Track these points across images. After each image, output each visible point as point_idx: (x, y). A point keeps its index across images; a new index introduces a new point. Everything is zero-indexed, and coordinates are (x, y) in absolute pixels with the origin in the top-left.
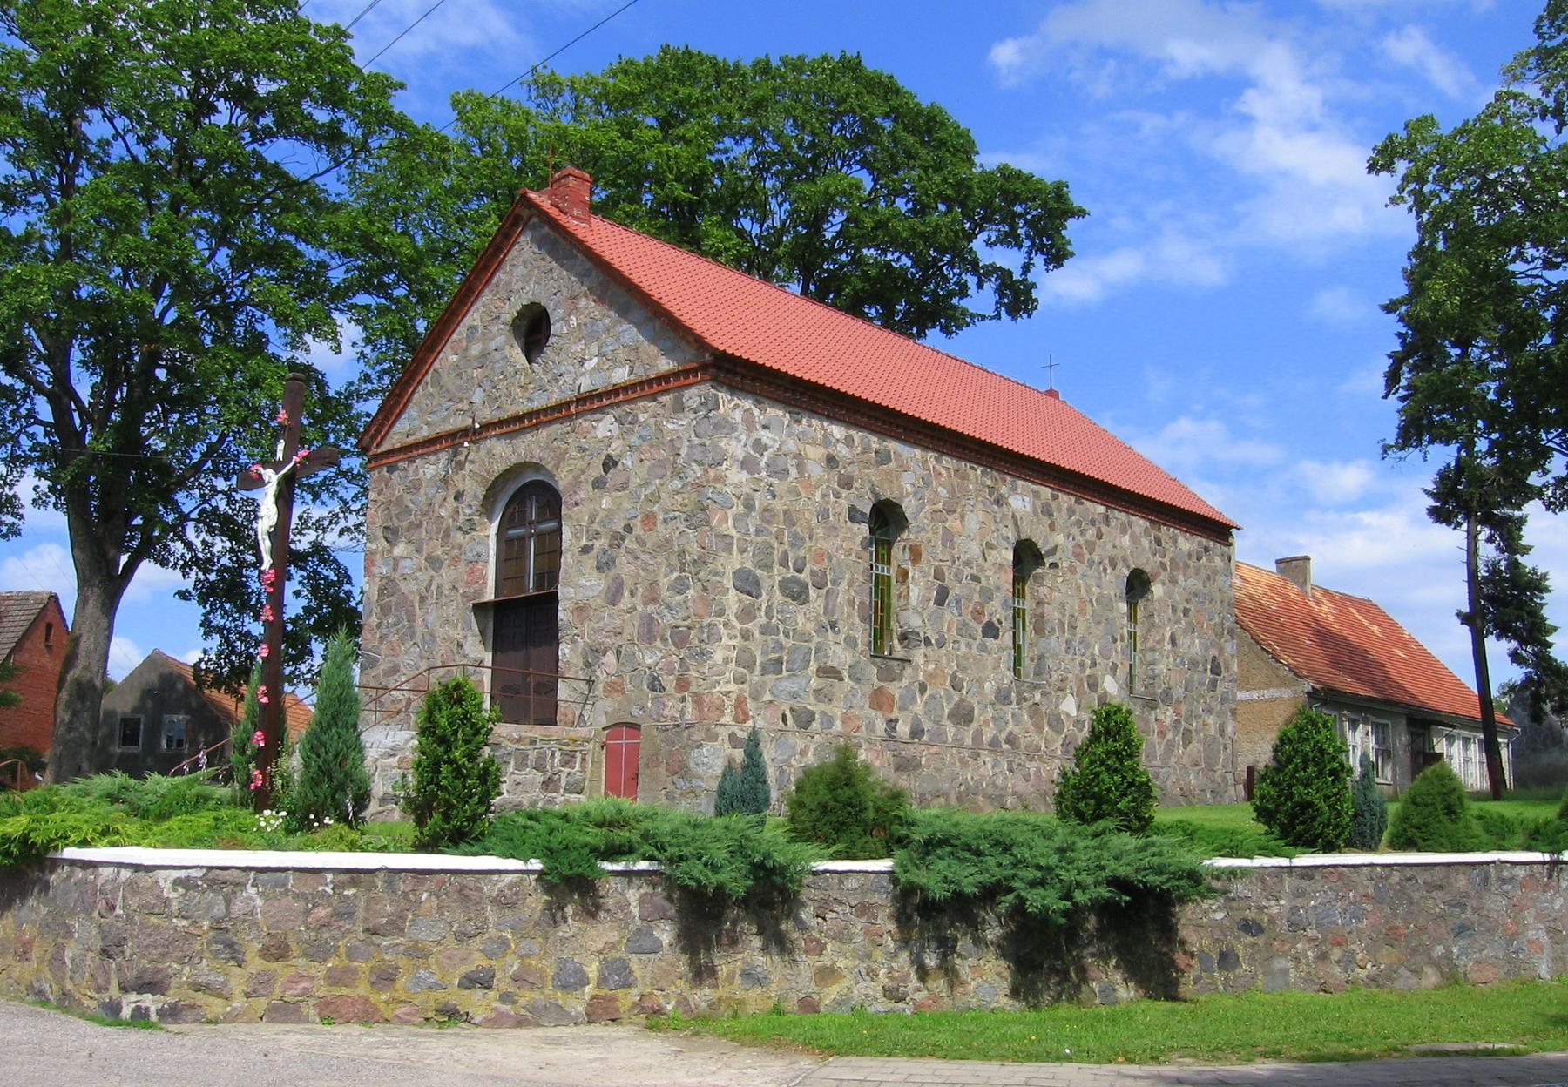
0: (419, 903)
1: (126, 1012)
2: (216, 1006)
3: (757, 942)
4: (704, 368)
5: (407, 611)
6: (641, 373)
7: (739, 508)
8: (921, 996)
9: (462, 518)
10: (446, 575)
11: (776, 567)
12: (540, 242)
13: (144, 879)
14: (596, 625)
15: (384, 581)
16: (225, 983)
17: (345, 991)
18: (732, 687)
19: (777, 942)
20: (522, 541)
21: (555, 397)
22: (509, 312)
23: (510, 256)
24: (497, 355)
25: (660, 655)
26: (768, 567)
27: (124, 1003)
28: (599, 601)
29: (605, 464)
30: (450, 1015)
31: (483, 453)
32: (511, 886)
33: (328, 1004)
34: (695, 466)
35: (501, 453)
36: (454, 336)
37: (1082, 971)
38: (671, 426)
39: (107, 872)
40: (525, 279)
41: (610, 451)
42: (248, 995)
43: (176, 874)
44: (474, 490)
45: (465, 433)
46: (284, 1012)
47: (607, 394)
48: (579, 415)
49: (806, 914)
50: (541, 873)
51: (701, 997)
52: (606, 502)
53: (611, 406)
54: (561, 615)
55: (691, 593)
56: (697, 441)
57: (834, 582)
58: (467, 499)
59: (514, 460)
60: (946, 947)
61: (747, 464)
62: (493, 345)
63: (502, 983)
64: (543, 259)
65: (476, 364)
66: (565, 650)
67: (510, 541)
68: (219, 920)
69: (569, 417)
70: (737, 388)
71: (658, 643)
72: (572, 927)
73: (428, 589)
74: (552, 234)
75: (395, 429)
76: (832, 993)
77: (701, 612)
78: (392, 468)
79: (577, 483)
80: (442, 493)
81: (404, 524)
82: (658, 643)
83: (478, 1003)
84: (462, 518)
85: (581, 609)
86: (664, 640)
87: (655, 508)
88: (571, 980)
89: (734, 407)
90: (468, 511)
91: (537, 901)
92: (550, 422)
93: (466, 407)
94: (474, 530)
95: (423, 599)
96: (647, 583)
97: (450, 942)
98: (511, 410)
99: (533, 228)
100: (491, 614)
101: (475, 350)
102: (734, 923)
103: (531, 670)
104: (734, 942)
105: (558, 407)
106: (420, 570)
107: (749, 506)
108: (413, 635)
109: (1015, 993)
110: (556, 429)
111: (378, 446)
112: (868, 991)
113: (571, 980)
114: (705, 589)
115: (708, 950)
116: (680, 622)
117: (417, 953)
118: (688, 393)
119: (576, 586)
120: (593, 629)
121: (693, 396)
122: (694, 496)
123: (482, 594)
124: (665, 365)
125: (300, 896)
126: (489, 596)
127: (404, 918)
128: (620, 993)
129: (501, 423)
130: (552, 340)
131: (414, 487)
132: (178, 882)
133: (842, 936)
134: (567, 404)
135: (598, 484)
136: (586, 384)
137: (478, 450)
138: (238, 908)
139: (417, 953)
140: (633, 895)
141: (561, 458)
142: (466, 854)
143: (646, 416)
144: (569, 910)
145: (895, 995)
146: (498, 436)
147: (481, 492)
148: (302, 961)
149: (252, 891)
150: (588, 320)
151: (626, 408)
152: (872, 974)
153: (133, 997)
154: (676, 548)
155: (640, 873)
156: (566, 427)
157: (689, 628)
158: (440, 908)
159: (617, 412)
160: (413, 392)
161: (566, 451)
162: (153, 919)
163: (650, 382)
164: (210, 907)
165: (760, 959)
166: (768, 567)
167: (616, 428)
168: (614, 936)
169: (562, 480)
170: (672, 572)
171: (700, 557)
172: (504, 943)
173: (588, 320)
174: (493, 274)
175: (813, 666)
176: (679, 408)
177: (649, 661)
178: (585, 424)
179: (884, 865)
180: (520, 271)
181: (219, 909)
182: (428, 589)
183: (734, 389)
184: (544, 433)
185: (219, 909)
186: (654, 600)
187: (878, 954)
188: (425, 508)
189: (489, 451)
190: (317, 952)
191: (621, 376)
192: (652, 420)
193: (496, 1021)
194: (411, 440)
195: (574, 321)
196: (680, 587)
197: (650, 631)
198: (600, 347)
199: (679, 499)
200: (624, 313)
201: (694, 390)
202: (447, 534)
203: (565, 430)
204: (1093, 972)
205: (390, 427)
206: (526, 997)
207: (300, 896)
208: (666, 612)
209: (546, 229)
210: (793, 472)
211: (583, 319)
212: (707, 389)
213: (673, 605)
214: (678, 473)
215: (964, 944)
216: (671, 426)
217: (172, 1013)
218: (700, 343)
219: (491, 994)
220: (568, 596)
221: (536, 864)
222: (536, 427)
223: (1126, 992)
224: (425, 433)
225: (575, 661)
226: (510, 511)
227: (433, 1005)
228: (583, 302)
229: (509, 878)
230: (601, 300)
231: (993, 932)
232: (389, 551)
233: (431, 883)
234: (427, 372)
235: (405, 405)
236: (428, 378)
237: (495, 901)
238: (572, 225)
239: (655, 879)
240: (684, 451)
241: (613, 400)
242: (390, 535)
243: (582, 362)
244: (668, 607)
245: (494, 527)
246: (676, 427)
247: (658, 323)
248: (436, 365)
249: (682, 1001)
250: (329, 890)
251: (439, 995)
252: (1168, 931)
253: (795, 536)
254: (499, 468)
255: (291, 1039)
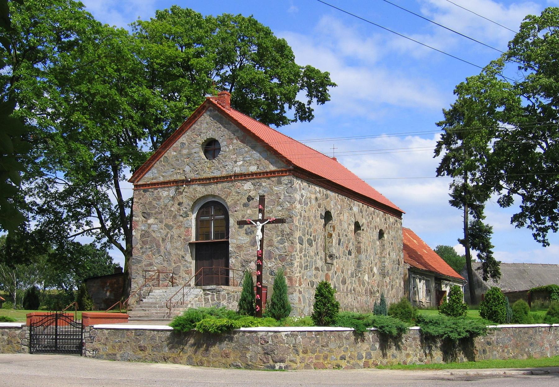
0: (331, 339)
1: (277, 368)
2: (294, 366)
3: (394, 347)
4: (290, 171)
5: (156, 244)
6: (262, 169)
7: (299, 217)
8: (426, 360)
9: (182, 212)
10: (175, 232)
11: (306, 235)
12: (214, 117)
13: (279, 335)
14: (246, 253)
15: (143, 232)
16: (296, 360)
17: (319, 361)
18: (299, 275)
19: (398, 348)
20: (209, 222)
21: (224, 174)
22: (201, 140)
23: (200, 119)
24: (196, 155)
25: (274, 264)
26: (304, 235)
27: (276, 365)
28: (247, 245)
29: (248, 199)
30: (339, 366)
31: (191, 189)
32: (348, 334)
33: (315, 364)
34: (287, 203)
35: (200, 191)
36: (174, 145)
37: (456, 354)
38: (276, 189)
39: (261, 334)
40: (208, 129)
41: (250, 194)
42: (300, 363)
43: (286, 333)
44: (187, 203)
45: (182, 181)
46: (307, 367)
47: (249, 175)
48: (235, 181)
49: (403, 340)
50: (354, 331)
51: (385, 361)
52: (249, 212)
53: (250, 179)
54: (230, 249)
55: (286, 244)
56: (287, 195)
57: (318, 239)
58: (185, 205)
59: (206, 193)
60: (430, 348)
61: (300, 202)
62: (194, 151)
63: (347, 359)
64: (216, 123)
65: (185, 157)
66: (232, 261)
67: (202, 221)
68: (294, 344)
69: (232, 181)
70: (298, 177)
71: (273, 260)
72: (360, 344)
73: (166, 236)
74: (220, 115)
75: (145, 176)
76: (409, 360)
77: (291, 251)
78: (145, 191)
79: (236, 204)
80: (172, 202)
81: (153, 212)
82: (273, 260)
83: (343, 363)
84: (182, 212)
85: (239, 247)
86: (275, 259)
87: (271, 215)
88: (360, 358)
89: (297, 183)
90: (185, 210)
91: (353, 338)
92: (223, 182)
93: (182, 172)
94: (188, 216)
95: (163, 240)
96: (268, 240)
97: (337, 348)
98: (204, 176)
99: (210, 111)
100: (194, 246)
101: (185, 152)
102: (390, 343)
103: (214, 267)
104: (390, 347)
105: (227, 177)
106: (162, 229)
107: (301, 216)
108: (159, 252)
109: (443, 360)
110: (226, 184)
111: (138, 182)
112: (416, 359)
113: (360, 358)
114: (292, 243)
115: (385, 349)
116: (282, 253)
117: (331, 351)
118: (283, 179)
119: (237, 239)
120: (245, 254)
121: (285, 179)
122: (287, 213)
123: (190, 239)
124: (272, 168)
125: (309, 338)
126: (193, 240)
127: (328, 343)
128: (369, 360)
129: (200, 180)
130: (221, 152)
131: (158, 199)
132: (286, 335)
133: (410, 346)
134: (231, 176)
135: (245, 205)
136: (238, 170)
137: (189, 188)
138: (297, 341)
139: (331, 351)
140: (371, 336)
141: (229, 194)
142: (336, 327)
143: (265, 184)
144: (359, 340)
145: (421, 360)
146: (199, 185)
147: (191, 203)
148: (310, 354)
149: (299, 337)
150: (238, 148)
151: (257, 180)
152: (416, 355)
153: (279, 364)
154: (280, 229)
155: (372, 330)
156: (230, 184)
157: (286, 256)
158: (335, 340)
159: (253, 181)
160: (155, 164)
161: (230, 193)
162: (281, 344)
163: (267, 173)
164: (292, 341)
165: (395, 352)
166: (304, 235)
167: (252, 187)
168: (368, 346)
169: (229, 202)
170: (278, 237)
171: (290, 233)
172: (347, 348)
173: (238, 148)
174: (192, 125)
175: (314, 267)
176: (280, 183)
177: (269, 266)
178: (239, 184)
179: (418, 328)
180: (205, 125)
181: (294, 342)
182: (166, 236)
183: (297, 177)
184: (220, 186)
185: (294, 342)
186: (271, 246)
187: (418, 351)
188: (163, 207)
189: (194, 189)
190: (313, 352)
191: (253, 169)
192: (268, 186)
193: (347, 368)
194: (154, 181)
195: (231, 147)
196: (282, 242)
197: (270, 256)
198: (243, 158)
199: (281, 213)
200: (253, 148)
201: (286, 178)
202: (175, 217)
203: (230, 185)
204: (458, 355)
205: (144, 175)
206: (352, 362)
207: (309, 338)
208: (276, 250)
209: (216, 112)
210: (309, 203)
211: (235, 147)
212: (291, 178)
213: (279, 248)
214: (280, 205)
215: (433, 348)
216: (276, 189)
217: (286, 367)
218: (289, 162)
219: (346, 361)
220: (233, 242)
221: (353, 329)
222: (217, 183)
223: (465, 360)
224: (161, 179)
225: (237, 264)
226: (202, 210)
227: (335, 364)
228: (235, 141)
229: (348, 332)
230: (242, 141)
231: (439, 345)
232: (147, 221)
233: (333, 333)
234: (161, 157)
235: (151, 168)
236: (162, 159)
237: (345, 338)
238: (228, 112)
239: (375, 332)
240: (282, 197)
241: (251, 177)
242: (145, 215)
243: (236, 162)
244: (277, 248)
245: (194, 216)
246: (278, 189)
247: (269, 153)
248: (166, 155)
249: (381, 362)
250: (314, 336)
251: (336, 361)
252: (472, 344)
253: (310, 224)
254: (199, 196)
255: (312, 372)
